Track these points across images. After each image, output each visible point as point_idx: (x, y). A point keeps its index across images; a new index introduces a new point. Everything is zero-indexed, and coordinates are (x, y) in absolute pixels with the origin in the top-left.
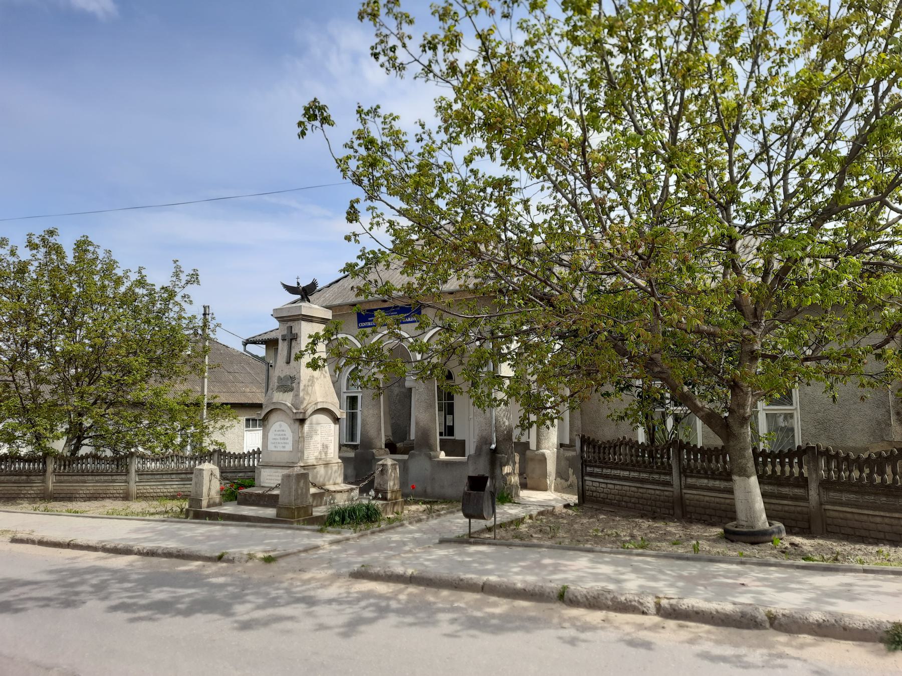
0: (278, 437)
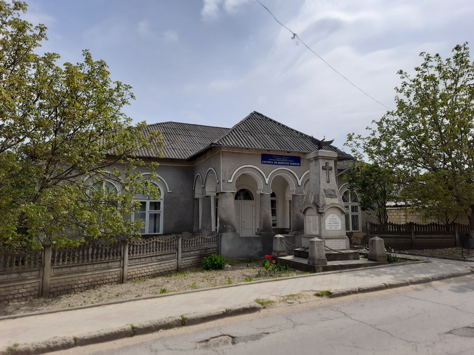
0: (332, 222)
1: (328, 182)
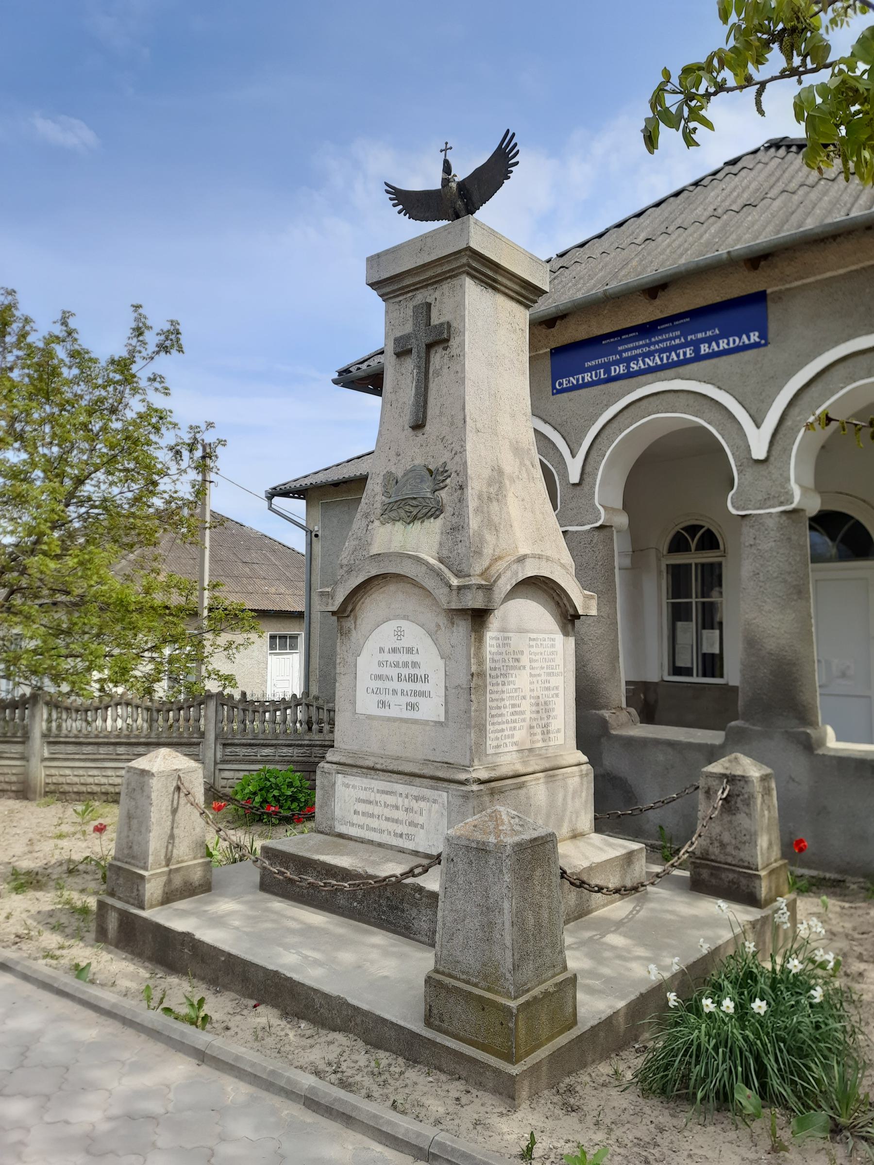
0: (393, 672)
1: (418, 426)
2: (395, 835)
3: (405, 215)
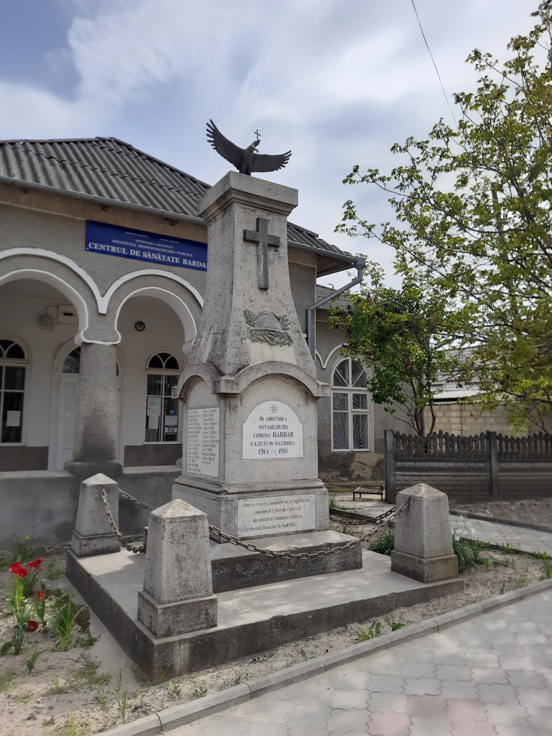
0: (271, 432)
1: (264, 289)
2: (284, 526)
3: (212, 145)
